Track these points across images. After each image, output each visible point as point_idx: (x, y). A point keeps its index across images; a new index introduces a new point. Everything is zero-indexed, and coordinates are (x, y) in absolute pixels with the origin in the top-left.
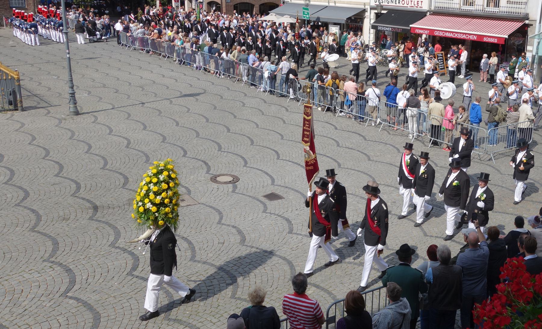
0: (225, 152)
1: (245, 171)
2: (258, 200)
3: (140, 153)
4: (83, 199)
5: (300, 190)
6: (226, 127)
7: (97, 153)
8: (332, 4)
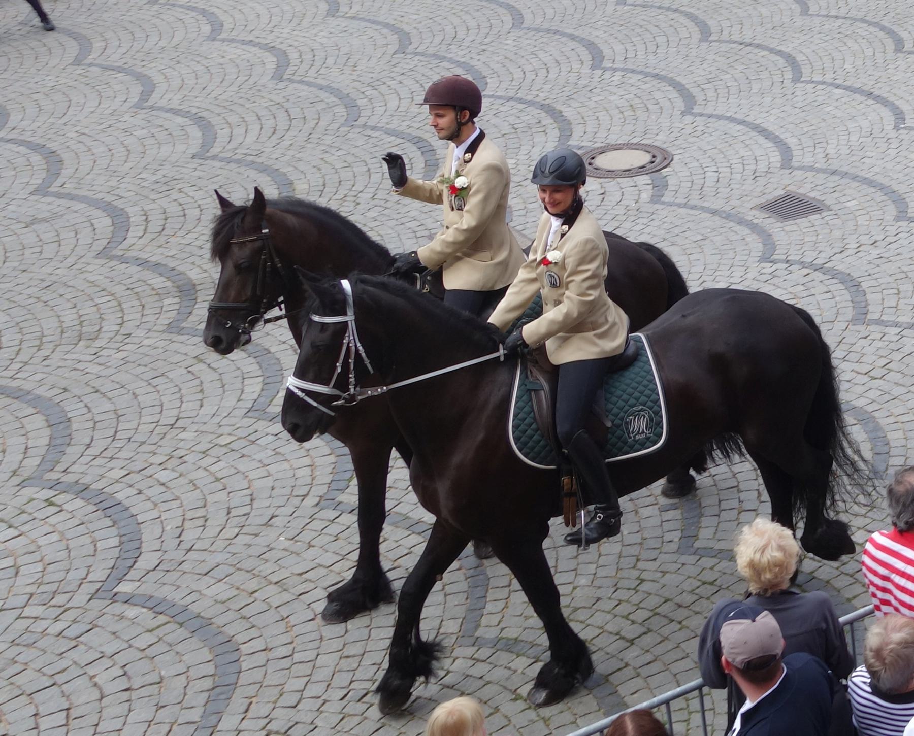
0: (615, 70)
1: (689, 130)
2: (741, 222)
3: (323, 95)
4: (143, 264)
5: (880, 179)
7: (175, 105)
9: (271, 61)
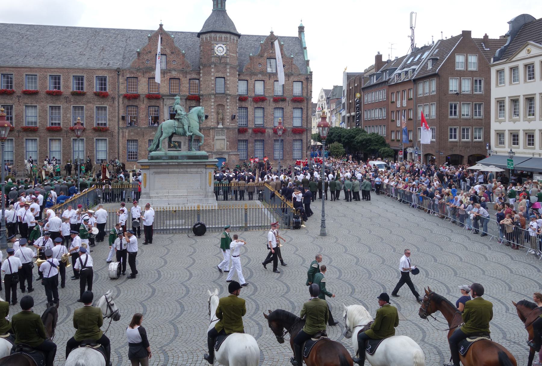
6: (433, 257)
8: (537, 156)
9: (355, 260)
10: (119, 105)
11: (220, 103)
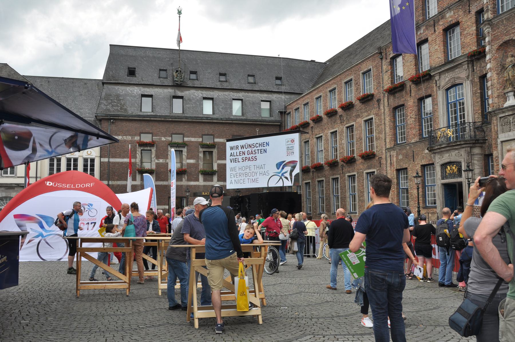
10: (385, 110)
11: (507, 38)
